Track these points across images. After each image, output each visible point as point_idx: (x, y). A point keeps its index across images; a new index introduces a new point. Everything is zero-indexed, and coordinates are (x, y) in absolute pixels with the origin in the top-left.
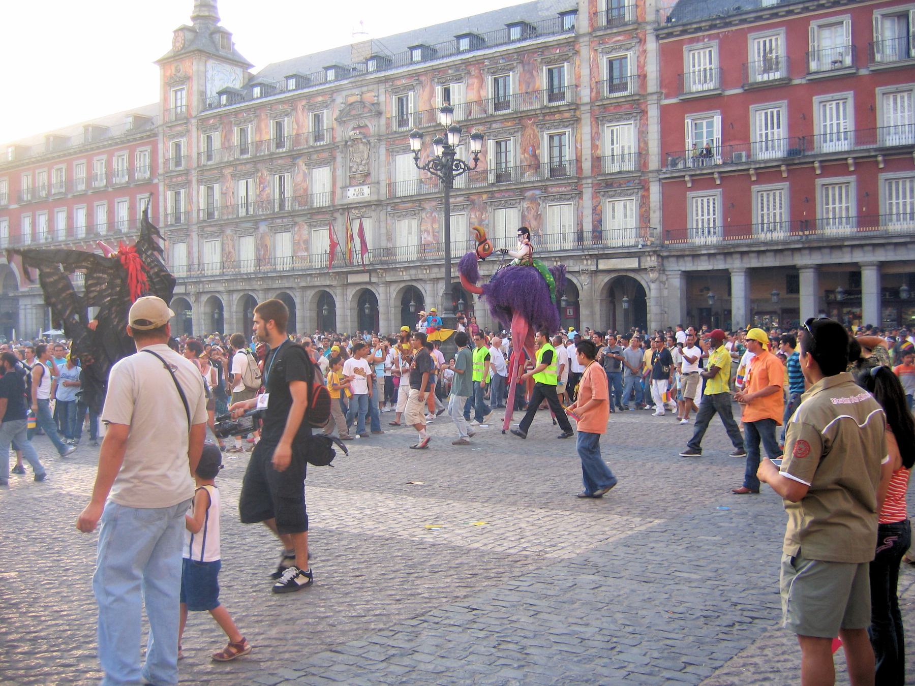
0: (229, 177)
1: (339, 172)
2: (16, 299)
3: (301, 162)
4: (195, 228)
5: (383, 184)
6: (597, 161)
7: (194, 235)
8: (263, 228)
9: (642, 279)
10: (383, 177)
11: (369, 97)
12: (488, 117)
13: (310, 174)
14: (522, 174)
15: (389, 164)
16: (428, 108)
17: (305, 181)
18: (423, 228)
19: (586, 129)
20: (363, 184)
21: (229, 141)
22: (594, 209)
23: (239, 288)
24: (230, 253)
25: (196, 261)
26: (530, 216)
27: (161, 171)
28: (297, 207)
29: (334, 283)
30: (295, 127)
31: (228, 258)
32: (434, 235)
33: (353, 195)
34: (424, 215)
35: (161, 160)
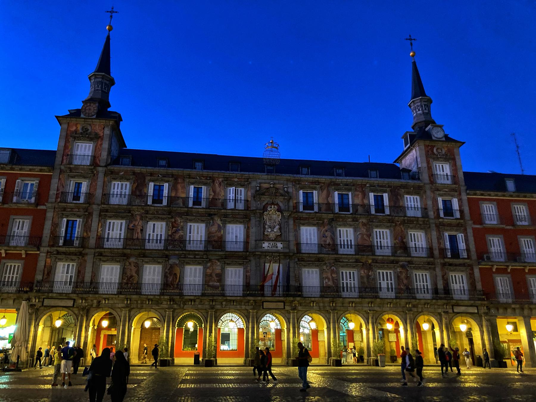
0: (138, 217)
1: (253, 230)
10: (292, 238)
13: (225, 227)
14: (396, 252)
16: (326, 202)
17: (220, 231)
18: (324, 276)
21: (140, 191)
22: (443, 276)
24: (132, 276)
26: (403, 276)
30: (213, 194)
32: (333, 282)
34: (325, 267)
35: (53, 192)
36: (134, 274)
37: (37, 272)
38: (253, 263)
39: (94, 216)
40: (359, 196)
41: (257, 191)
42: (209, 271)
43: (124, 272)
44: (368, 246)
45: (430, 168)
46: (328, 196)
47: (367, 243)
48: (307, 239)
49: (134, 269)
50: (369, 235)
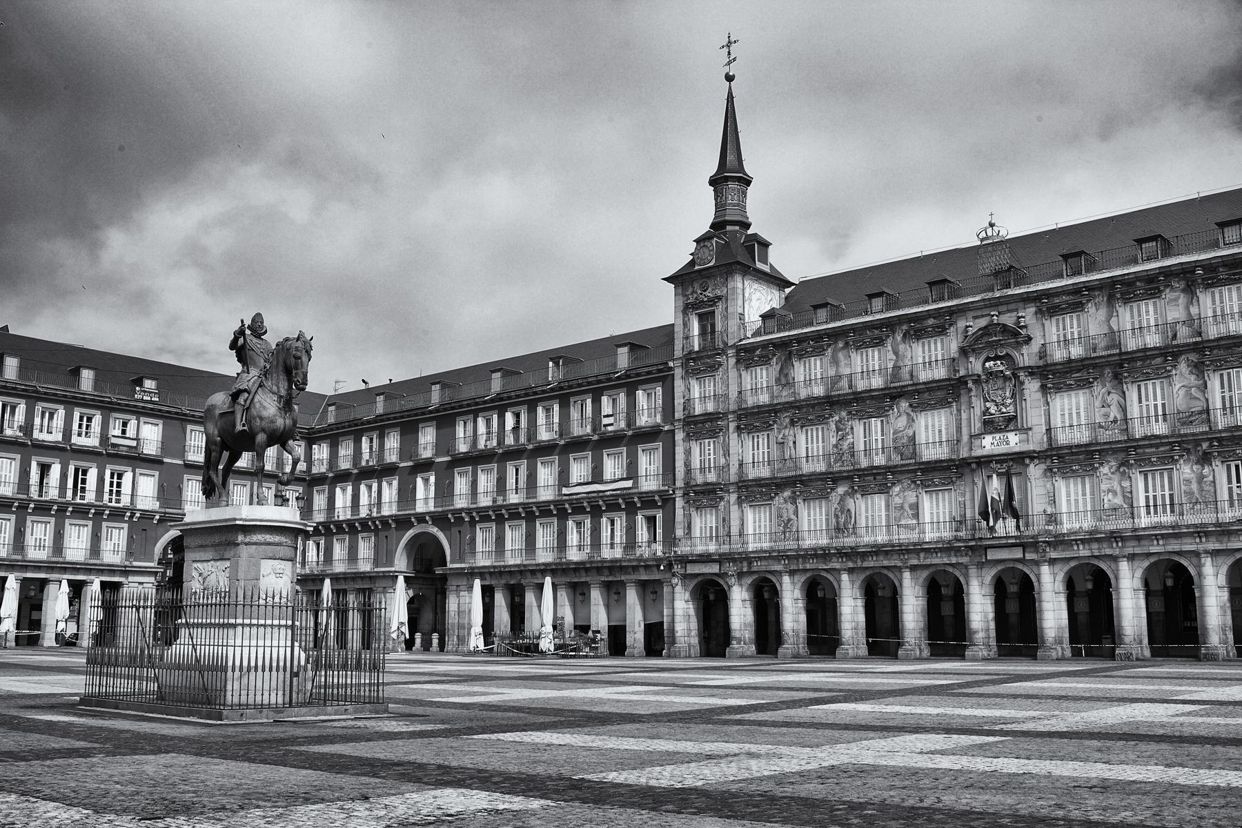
2: (444, 578)
3: (904, 405)
7: (733, 498)
11: (1008, 320)
12: (1202, 342)
20: (1004, 430)
21: (786, 375)
23: (808, 566)
24: (789, 520)
25: (735, 530)
27: (679, 414)
28: (896, 460)
29: (964, 560)
31: (787, 526)
33: (990, 444)
34: (1105, 470)
35: (679, 401)
36: (793, 517)
37: (677, 526)
39: (731, 429)
40: (1180, 301)
42: (898, 500)
44: (1200, 413)
46: (1110, 317)
47: (1198, 406)
48: (1070, 414)
49: (791, 508)
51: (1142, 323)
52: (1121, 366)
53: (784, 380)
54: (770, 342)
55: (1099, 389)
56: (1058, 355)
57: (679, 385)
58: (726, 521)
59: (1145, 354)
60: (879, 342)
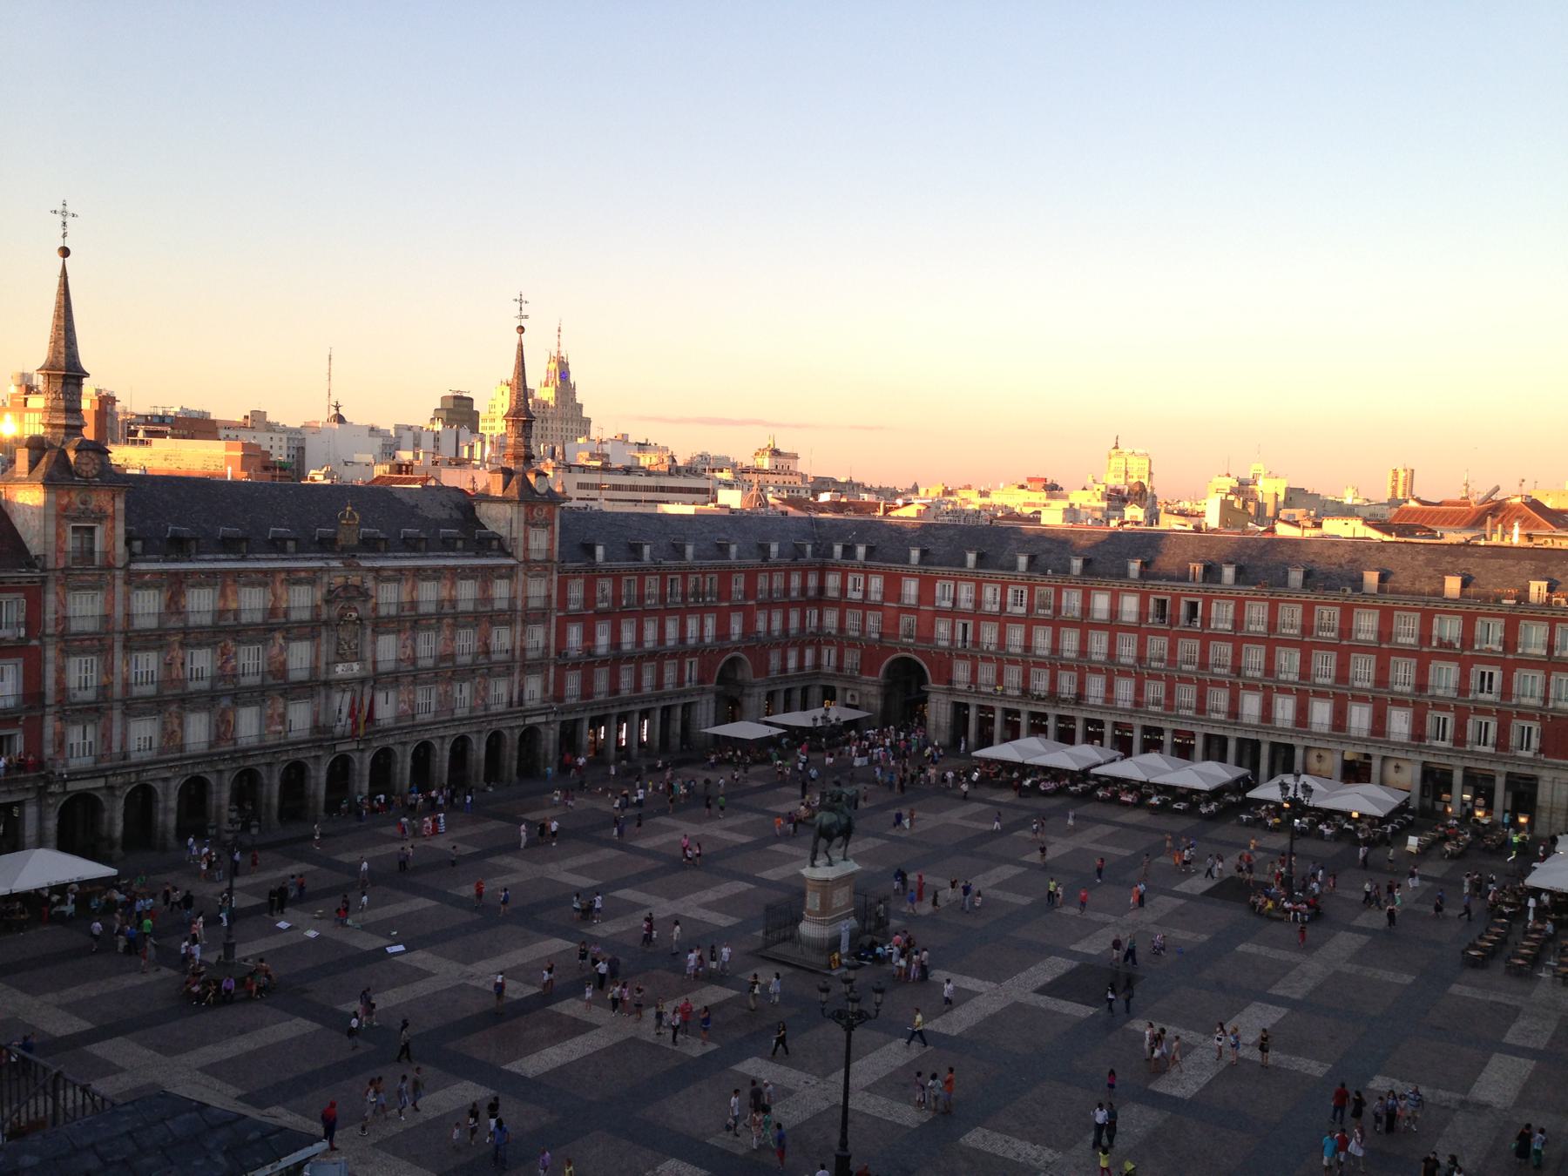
0: (176, 646)
1: (323, 648)
3: (279, 637)
4: (118, 705)
5: (370, 660)
6: (523, 650)
7: (117, 715)
8: (225, 702)
9: (542, 729)
10: (368, 655)
15: (374, 643)
19: (519, 628)
21: (176, 603)
28: (270, 681)
33: (340, 669)
35: (50, 616)
38: (323, 693)
41: (330, 592)
43: (164, 729)
45: (526, 539)
49: (176, 721)
50: (453, 639)
51: (429, 593)
52: (416, 622)
53: (174, 605)
54: (167, 572)
55: (403, 636)
56: (383, 611)
57: (51, 600)
58: (106, 737)
59: (427, 616)
60: (264, 585)
